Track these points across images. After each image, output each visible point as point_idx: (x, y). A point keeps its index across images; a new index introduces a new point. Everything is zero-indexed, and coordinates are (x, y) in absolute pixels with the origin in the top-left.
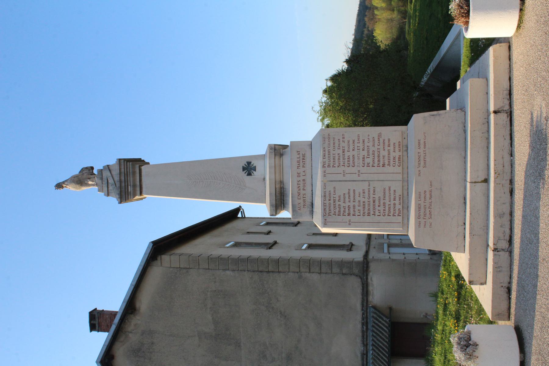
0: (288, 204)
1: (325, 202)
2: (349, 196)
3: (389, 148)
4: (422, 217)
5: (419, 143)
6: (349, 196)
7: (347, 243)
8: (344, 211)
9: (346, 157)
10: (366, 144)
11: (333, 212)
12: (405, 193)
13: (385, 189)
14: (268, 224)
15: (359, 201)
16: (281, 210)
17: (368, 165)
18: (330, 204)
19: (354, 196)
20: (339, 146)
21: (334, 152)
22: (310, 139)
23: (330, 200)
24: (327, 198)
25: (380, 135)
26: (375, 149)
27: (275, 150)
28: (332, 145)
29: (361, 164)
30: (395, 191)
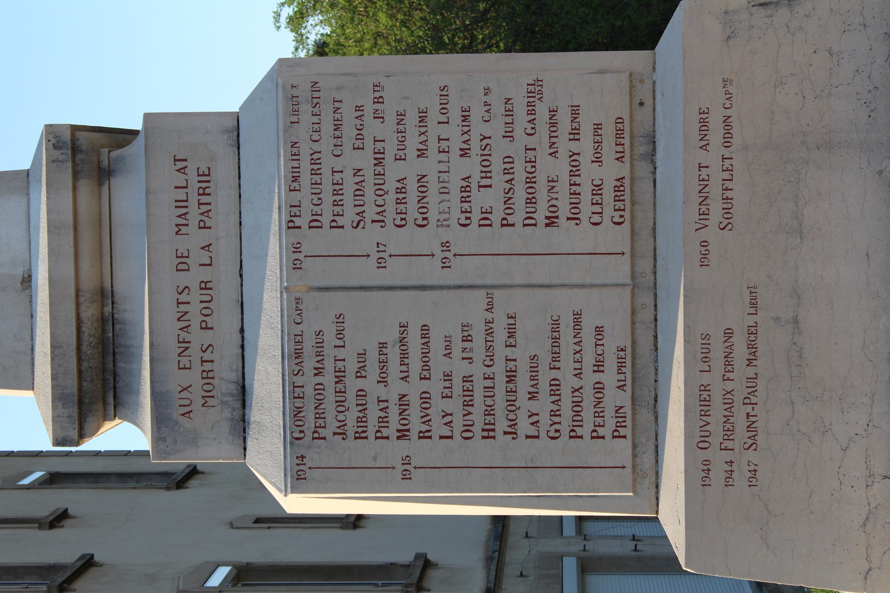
0: (137, 392)
1: (299, 380)
2: (404, 355)
3: (574, 146)
4: (716, 439)
5: (704, 123)
6: (404, 355)
7: (407, 557)
8: (383, 421)
9: (391, 185)
10: (478, 128)
11: (333, 425)
13: (556, 323)
14: (54, 479)
15: (448, 377)
16: (106, 418)
17: (485, 221)
18: (319, 388)
19: (425, 355)
20: (360, 137)
21: (338, 164)
22: (234, 106)
23: (318, 372)
24: (310, 363)
25: (535, 90)
26: (516, 149)
27: (75, 149)
28: (327, 128)
29: (456, 214)
30: (599, 330)
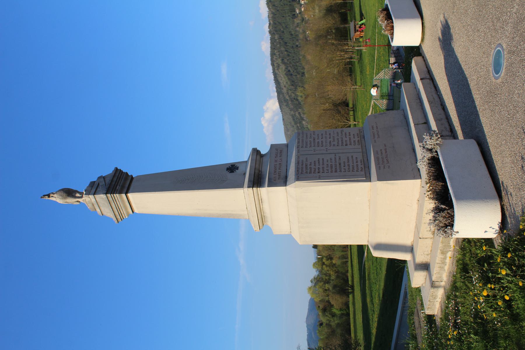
12: (365, 159)
24: (300, 164)
